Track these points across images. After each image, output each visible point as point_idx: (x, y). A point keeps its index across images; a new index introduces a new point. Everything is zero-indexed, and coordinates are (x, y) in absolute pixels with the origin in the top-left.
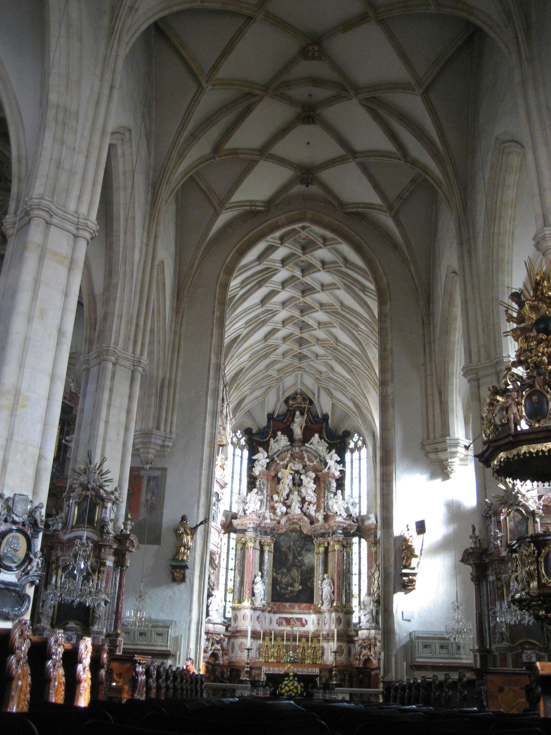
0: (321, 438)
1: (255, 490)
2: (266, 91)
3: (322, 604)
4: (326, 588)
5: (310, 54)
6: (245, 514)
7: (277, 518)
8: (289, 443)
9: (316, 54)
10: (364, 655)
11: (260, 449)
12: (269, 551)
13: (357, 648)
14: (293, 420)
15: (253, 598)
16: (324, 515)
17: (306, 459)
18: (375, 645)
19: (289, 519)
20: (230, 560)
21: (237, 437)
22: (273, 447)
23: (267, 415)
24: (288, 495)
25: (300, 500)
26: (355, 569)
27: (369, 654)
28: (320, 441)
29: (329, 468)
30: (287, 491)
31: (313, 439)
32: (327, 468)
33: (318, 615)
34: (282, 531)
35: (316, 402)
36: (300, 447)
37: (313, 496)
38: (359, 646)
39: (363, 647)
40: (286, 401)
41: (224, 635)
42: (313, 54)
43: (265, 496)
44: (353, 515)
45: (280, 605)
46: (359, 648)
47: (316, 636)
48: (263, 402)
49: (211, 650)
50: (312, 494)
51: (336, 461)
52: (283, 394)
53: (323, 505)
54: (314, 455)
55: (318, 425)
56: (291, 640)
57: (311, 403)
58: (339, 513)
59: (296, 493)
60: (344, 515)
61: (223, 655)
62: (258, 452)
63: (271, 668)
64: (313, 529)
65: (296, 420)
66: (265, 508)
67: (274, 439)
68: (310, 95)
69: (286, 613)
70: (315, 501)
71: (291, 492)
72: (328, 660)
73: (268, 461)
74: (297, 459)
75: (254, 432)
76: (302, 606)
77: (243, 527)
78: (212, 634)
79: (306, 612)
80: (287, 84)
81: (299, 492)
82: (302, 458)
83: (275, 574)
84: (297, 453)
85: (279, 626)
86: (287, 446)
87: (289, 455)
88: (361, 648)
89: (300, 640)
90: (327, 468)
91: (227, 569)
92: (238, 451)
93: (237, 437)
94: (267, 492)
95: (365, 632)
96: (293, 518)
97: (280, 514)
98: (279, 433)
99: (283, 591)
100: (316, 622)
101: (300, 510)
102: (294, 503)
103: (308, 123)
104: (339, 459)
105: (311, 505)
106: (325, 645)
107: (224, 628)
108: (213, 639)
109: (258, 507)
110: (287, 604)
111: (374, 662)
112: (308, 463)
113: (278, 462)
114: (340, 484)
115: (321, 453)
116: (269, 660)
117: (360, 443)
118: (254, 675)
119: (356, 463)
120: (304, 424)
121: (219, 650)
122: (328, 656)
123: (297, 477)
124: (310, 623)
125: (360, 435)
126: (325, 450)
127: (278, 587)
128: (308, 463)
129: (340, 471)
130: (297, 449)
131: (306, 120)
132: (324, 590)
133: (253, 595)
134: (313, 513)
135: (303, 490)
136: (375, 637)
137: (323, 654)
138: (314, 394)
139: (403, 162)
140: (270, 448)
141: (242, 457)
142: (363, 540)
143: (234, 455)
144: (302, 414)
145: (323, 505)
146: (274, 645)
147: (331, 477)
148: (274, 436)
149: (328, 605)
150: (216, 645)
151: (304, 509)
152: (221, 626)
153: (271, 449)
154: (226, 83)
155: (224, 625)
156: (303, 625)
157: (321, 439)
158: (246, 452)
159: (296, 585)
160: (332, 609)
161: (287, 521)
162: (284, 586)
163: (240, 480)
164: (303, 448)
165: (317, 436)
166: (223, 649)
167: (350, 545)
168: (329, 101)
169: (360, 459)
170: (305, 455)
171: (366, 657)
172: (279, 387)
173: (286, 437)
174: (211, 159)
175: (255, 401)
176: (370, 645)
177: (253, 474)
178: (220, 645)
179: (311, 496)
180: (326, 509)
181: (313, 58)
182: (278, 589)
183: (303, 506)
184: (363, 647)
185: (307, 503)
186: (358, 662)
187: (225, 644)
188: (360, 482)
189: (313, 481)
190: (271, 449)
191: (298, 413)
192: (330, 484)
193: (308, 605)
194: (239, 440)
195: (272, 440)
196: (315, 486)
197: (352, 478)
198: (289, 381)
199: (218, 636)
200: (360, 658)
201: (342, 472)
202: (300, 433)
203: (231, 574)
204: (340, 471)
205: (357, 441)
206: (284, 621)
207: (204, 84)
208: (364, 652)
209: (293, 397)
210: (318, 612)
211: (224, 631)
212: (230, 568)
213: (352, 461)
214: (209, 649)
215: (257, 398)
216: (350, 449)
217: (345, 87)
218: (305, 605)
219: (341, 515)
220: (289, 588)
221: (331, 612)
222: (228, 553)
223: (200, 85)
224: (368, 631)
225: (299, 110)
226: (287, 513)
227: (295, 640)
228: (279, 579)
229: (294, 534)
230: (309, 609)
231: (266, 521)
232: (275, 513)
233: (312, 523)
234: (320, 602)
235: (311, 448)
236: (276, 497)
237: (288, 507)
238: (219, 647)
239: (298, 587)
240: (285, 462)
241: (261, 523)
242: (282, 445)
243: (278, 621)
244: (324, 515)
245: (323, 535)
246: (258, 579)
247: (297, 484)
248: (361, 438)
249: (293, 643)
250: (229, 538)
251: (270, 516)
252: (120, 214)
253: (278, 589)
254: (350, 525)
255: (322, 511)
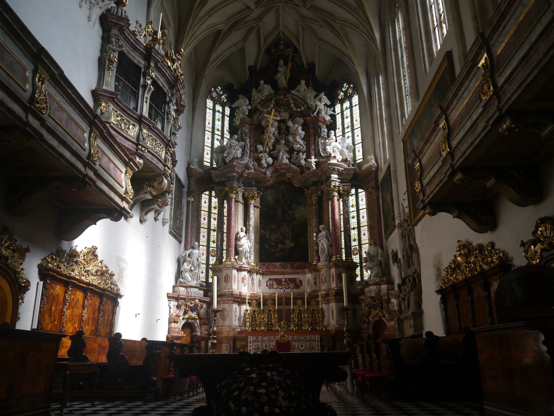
0: (307, 85)
1: (236, 137)
3: (319, 260)
4: (322, 241)
6: (224, 161)
7: (263, 170)
8: (273, 92)
10: (374, 316)
11: (240, 96)
12: (255, 206)
13: (364, 309)
14: (277, 72)
15: (237, 257)
16: (315, 162)
17: (292, 105)
18: (389, 301)
19: (275, 171)
20: (212, 220)
21: (217, 93)
22: (256, 96)
23: (249, 67)
24: (274, 146)
25: (287, 149)
26: (353, 222)
27: (380, 314)
28: (306, 88)
29: (319, 113)
30: (272, 141)
31: (299, 86)
32: (316, 112)
33: (314, 273)
34: (268, 184)
35: (301, 49)
36: (285, 95)
37: (302, 144)
38: (367, 305)
39: (371, 307)
40: (268, 51)
41: (200, 301)
43: (249, 146)
44: (349, 159)
45: (269, 265)
46: (367, 309)
47: (313, 296)
48: (242, 50)
49: (183, 319)
50: (301, 142)
51: (325, 105)
52: (265, 40)
53: (313, 152)
54: (301, 104)
55: (304, 73)
56: (284, 303)
57: (296, 50)
58: (333, 155)
59: (284, 142)
60: (339, 158)
61: (200, 325)
62: (238, 98)
63: (260, 338)
64: (304, 179)
65: (280, 69)
66: (248, 158)
67: (256, 90)
69: (276, 273)
70: (305, 149)
71: (277, 141)
72: (329, 325)
73: (250, 107)
74: (282, 107)
75: (236, 87)
76: (295, 265)
77: (223, 179)
78: (184, 299)
79: (300, 271)
81: (287, 141)
82: (287, 105)
83: (262, 231)
84: (282, 100)
85: (270, 288)
86: (271, 95)
87: (273, 102)
88: (370, 308)
89: (295, 304)
90: (316, 112)
91: (209, 229)
92: (219, 108)
93: (217, 93)
94: (250, 142)
95: (373, 288)
96: (281, 169)
97: (265, 165)
98: (262, 82)
99: (273, 250)
100: (312, 281)
101: (287, 160)
102: (281, 153)
104: (329, 103)
105: (301, 154)
106: (325, 307)
107: (202, 292)
108: (186, 305)
109: (239, 154)
110: (278, 264)
111: (388, 324)
112: (295, 109)
113: (262, 109)
114: (332, 126)
115: (308, 101)
116: (257, 328)
117: (350, 91)
118: (238, 347)
119: (347, 113)
120: (289, 75)
121: (194, 319)
122: (329, 319)
123: (283, 127)
124: (305, 283)
125: (349, 84)
126: (312, 98)
127: (266, 245)
128: (295, 109)
129: (330, 115)
130: (282, 97)
132: (320, 244)
133: (237, 253)
134: (303, 162)
135: (290, 138)
136: (388, 293)
137: (323, 317)
138: (298, 41)
140: (252, 99)
141: (223, 113)
142: (360, 190)
143: (214, 110)
144: (286, 64)
145: (313, 152)
146: (263, 310)
147: (321, 122)
148: (257, 86)
149: (326, 261)
150: (190, 312)
151: (292, 160)
152: (197, 289)
153: (254, 100)
155: (200, 289)
156: (297, 287)
157: (308, 88)
158: (228, 111)
159: (288, 242)
160: (332, 263)
161: (273, 172)
162: (273, 244)
163: (222, 136)
164: (288, 96)
165: (303, 82)
166: (200, 318)
167: (348, 194)
169: (351, 107)
170: (292, 101)
171: (377, 319)
172: (259, 30)
173: (269, 86)
175: (233, 48)
176: (381, 303)
177: (234, 124)
178: (195, 313)
179: (299, 142)
180: (318, 157)
182: (267, 247)
183: (291, 157)
184: (371, 307)
185: (295, 153)
186: (366, 326)
187: (202, 311)
188: (353, 130)
189: (300, 128)
190: (254, 100)
191: (281, 62)
192: (321, 130)
193: (302, 263)
194: (220, 96)
195: (254, 90)
196: (304, 133)
197: (343, 129)
198: (269, 22)
199: (192, 302)
200: (369, 320)
201: (333, 117)
202: (284, 83)
203: (214, 234)
204: (330, 115)
205: (347, 90)
206: (274, 283)
208: (374, 312)
209: (275, 44)
210: (315, 269)
211: (202, 296)
212: (212, 227)
213: (342, 112)
214: (181, 318)
215: (235, 45)
216: (339, 99)
218: (298, 263)
219: (335, 157)
220: (280, 246)
221: (330, 268)
222: (210, 212)
224: (378, 287)
226: (273, 164)
227: (288, 304)
228: (268, 236)
229: (282, 186)
230: (304, 267)
231: (250, 171)
232: (260, 165)
233: (302, 172)
234: (316, 258)
235: (298, 96)
236: (260, 148)
237: (275, 158)
238: (194, 315)
239: (289, 244)
240: (270, 108)
241: (243, 172)
242: (266, 94)
243: (268, 283)
244: (315, 162)
245: (315, 184)
246: (242, 234)
247: (284, 131)
248: (352, 85)
249: (286, 307)
250: (210, 196)
251: (253, 165)
253: (267, 247)
254: (345, 169)
255: (313, 157)
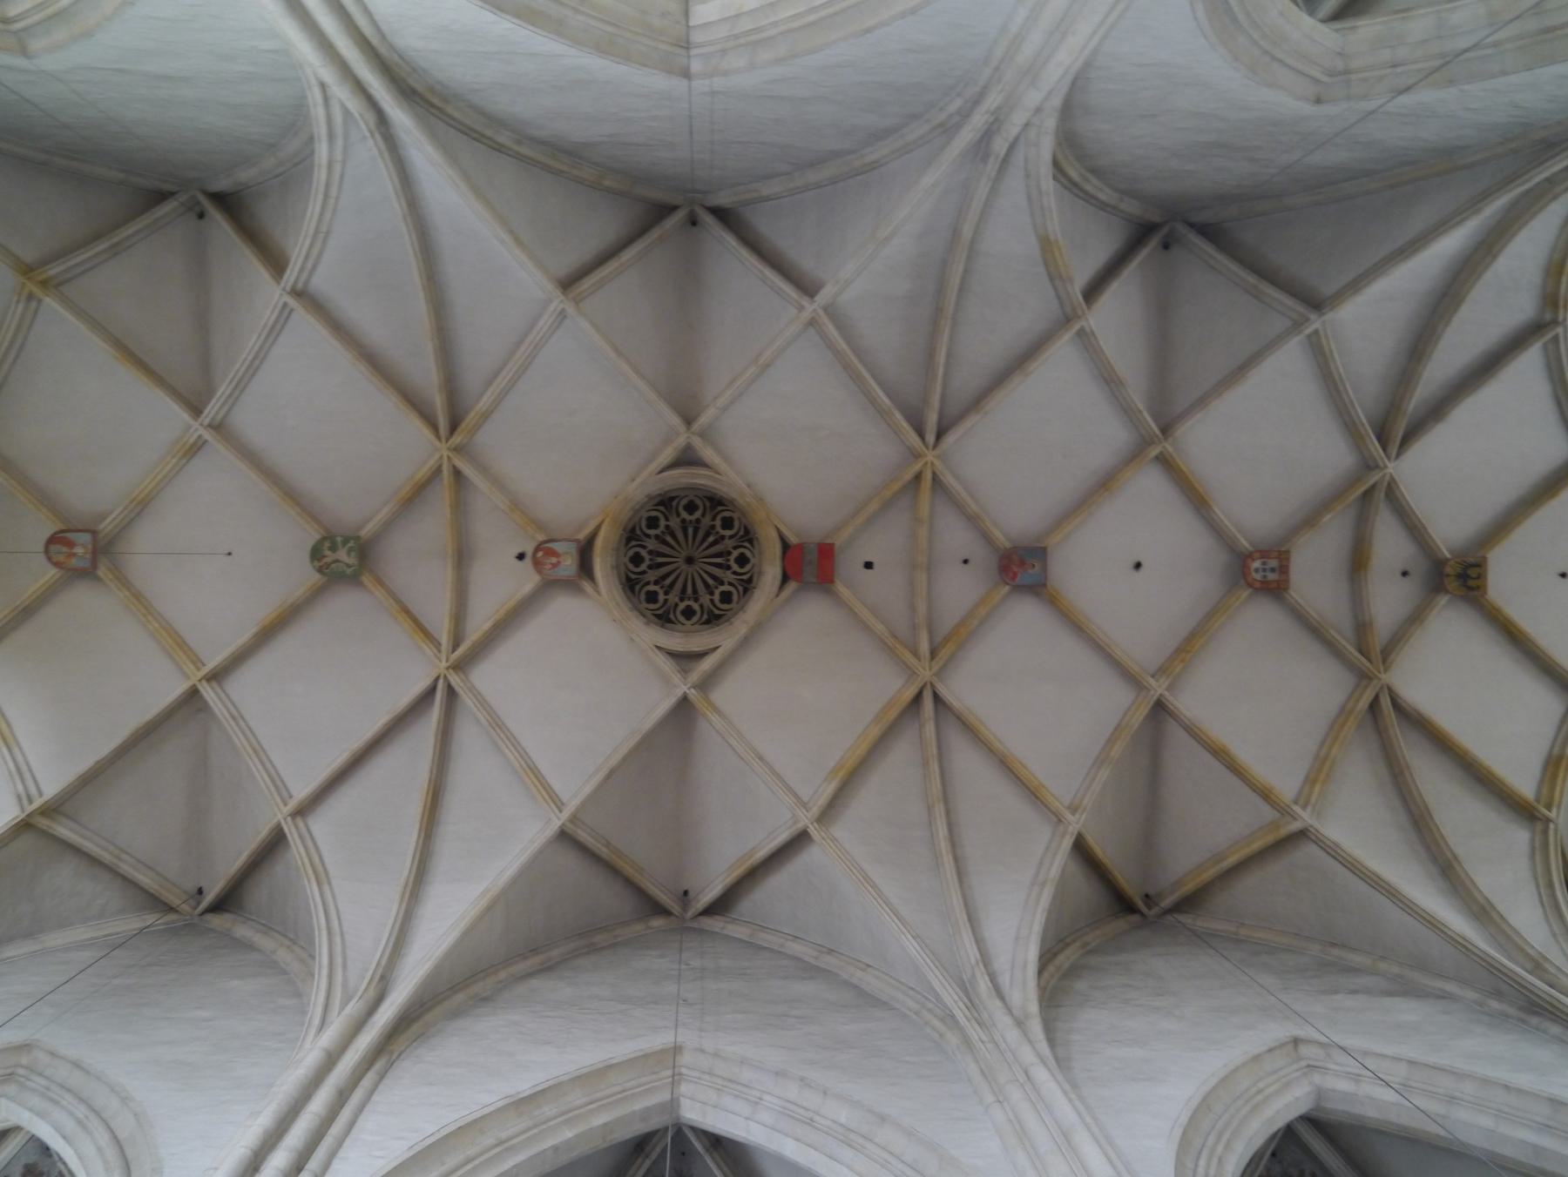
2: (1371, 679)
5: (1271, 576)
9: (1273, 563)
42: (1273, 570)
68: (1405, 574)
80: (1362, 628)
103: (1482, 577)
131: (1471, 583)
139: (1560, 330)
154: (1320, 772)
168: (1414, 529)
174: (1545, 832)
181: (1284, 569)
207: (1295, 826)
217: (1367, 495)
223: (1303, 835)
225: (1443, 600)
252: (1523, 1142)
